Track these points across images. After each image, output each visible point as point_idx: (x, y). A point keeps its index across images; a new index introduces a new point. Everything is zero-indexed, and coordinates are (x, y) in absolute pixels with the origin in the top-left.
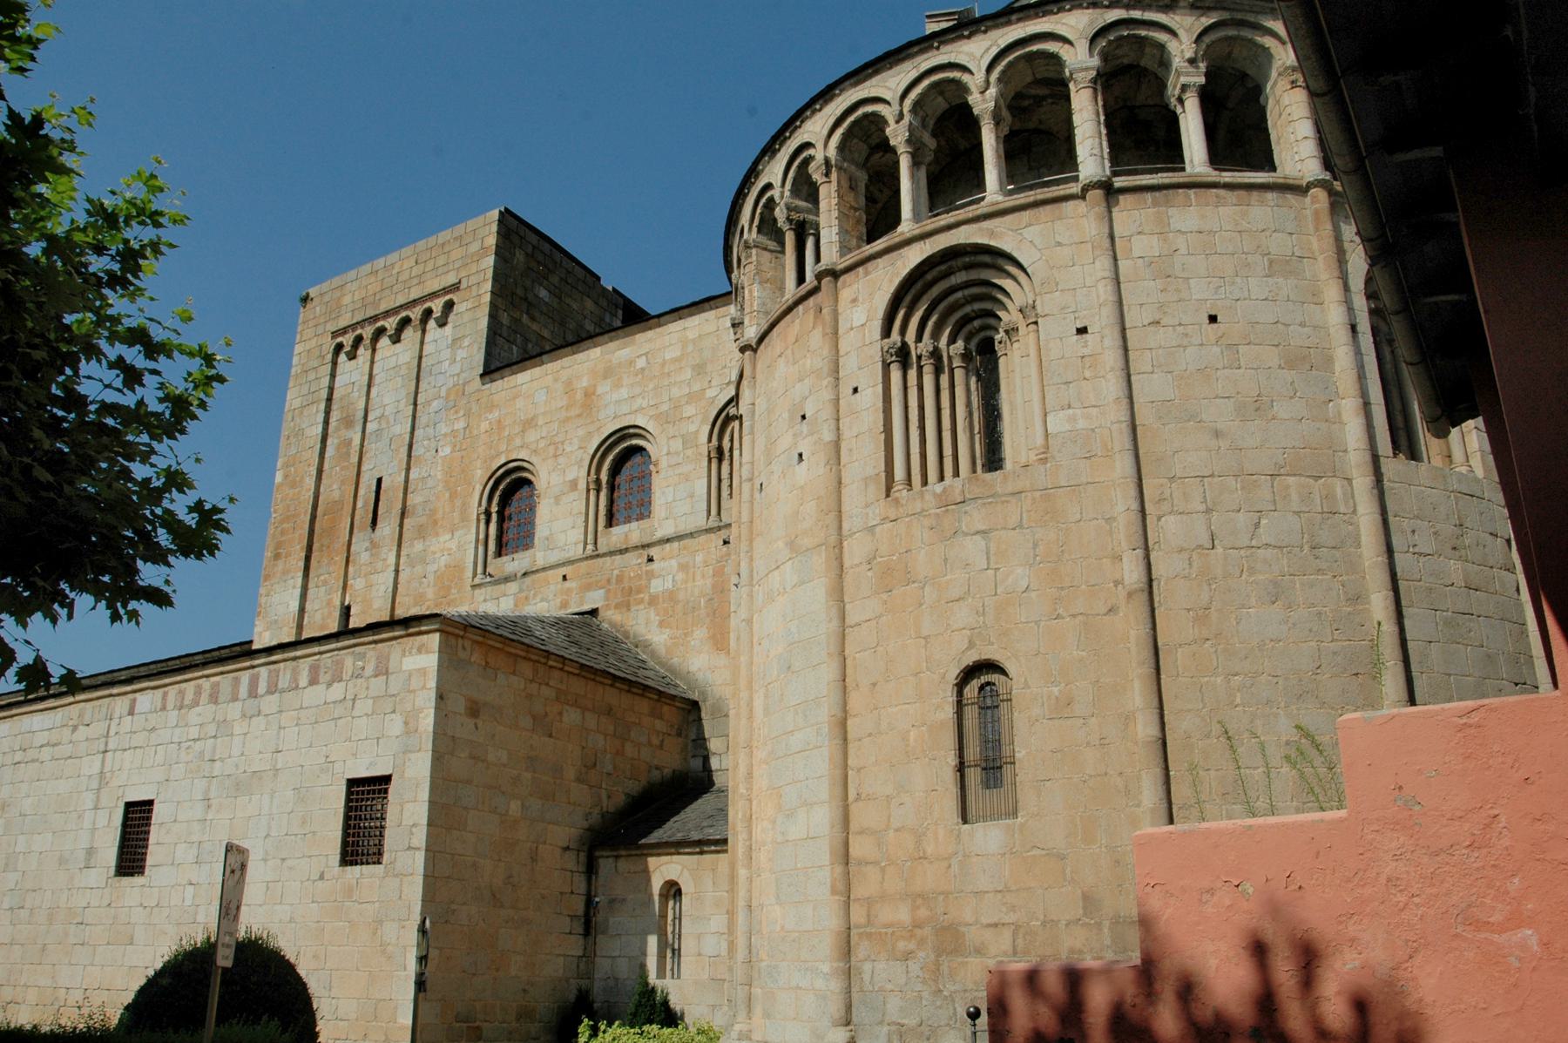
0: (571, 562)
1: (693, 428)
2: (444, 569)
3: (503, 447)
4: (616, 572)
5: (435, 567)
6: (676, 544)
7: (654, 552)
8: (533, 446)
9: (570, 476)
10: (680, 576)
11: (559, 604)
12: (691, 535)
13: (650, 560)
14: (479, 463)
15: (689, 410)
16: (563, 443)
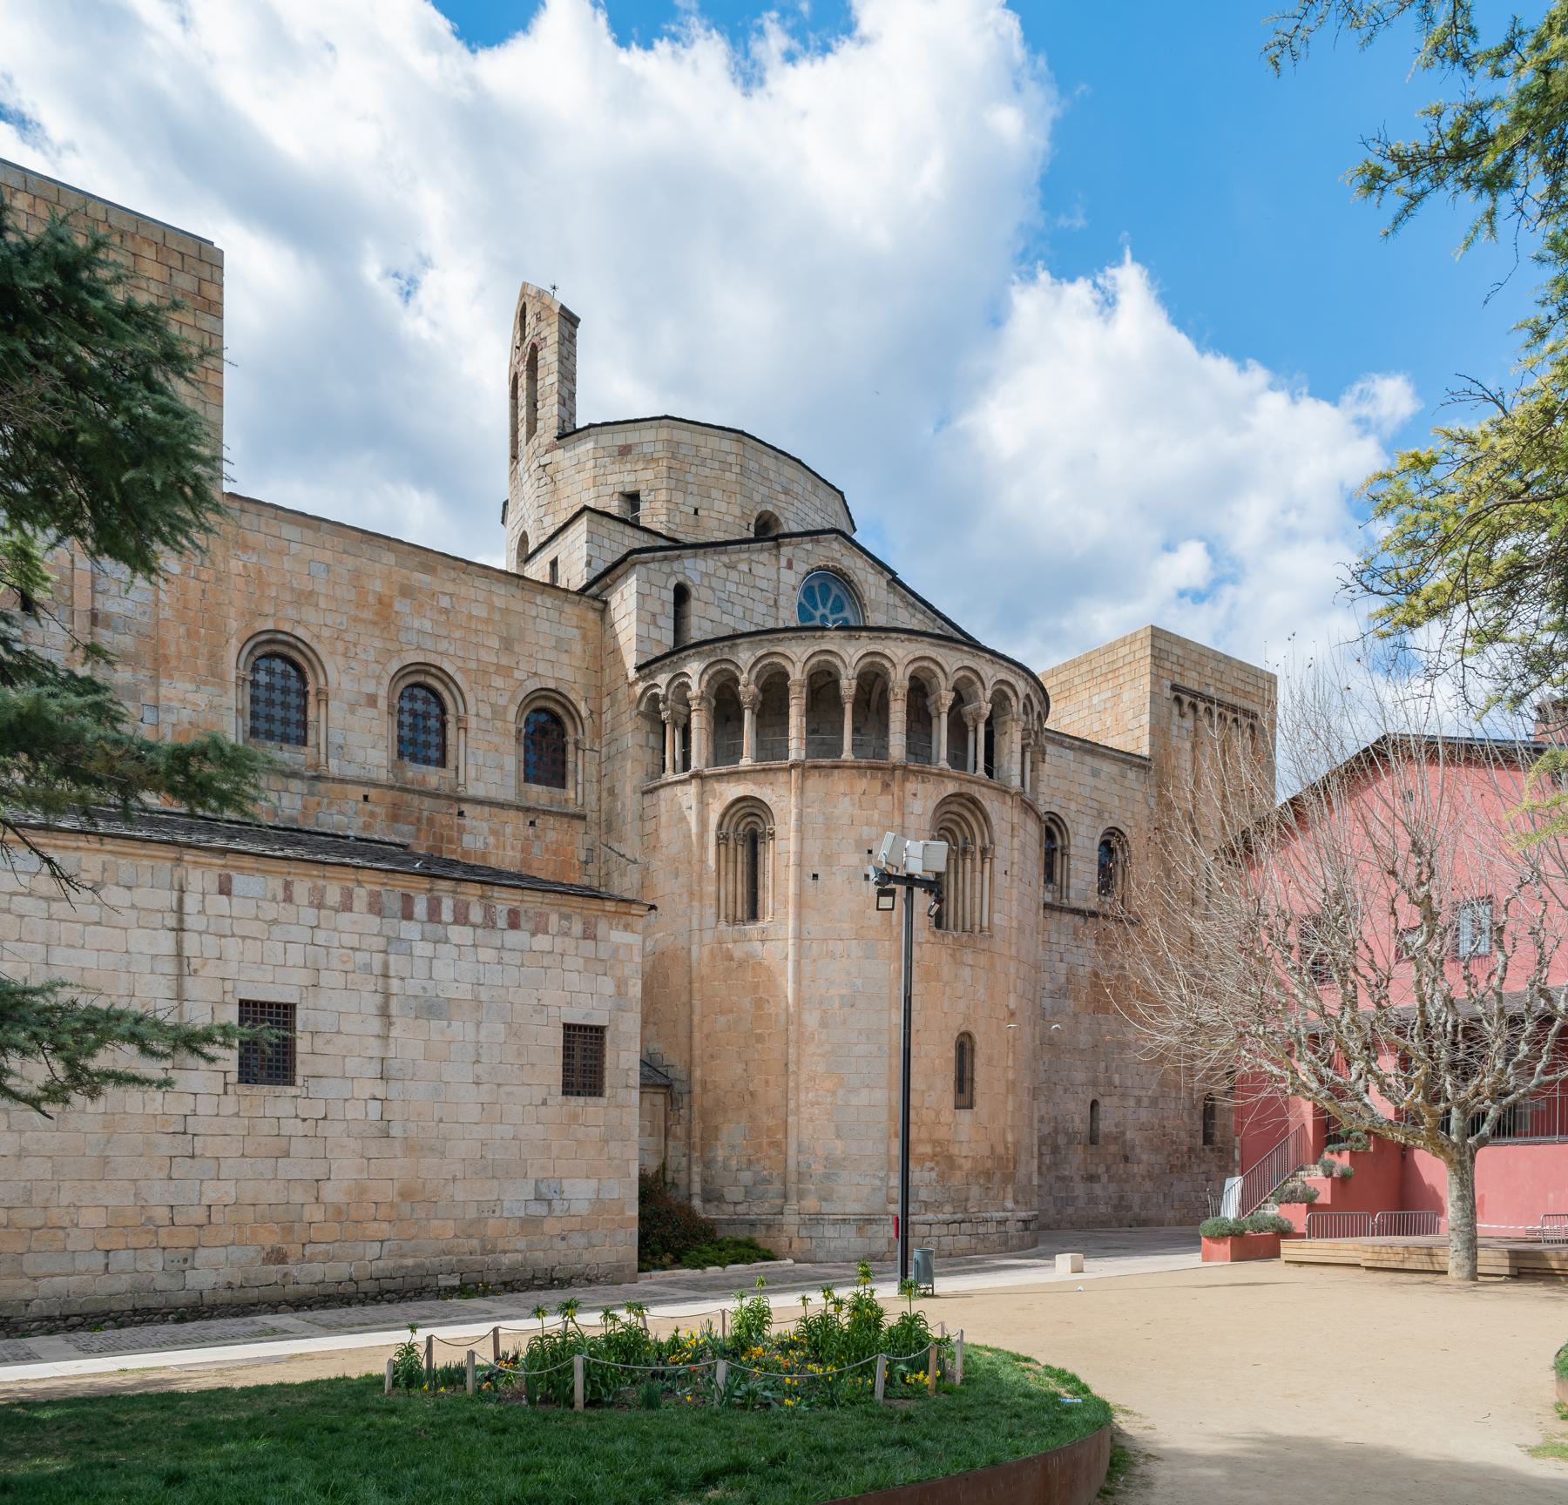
0: (374, 784)
1: (502, 701)
2: (186, 726)
3: (268, 608)
4: (425, 813)
5: (173, 718)
6: (486, 809)
7: (465, 807)
8: (316, 630)
9: (370, 687)
10: (491, 840)
11: (361, 824)
12: (502, 806)
13: (461, 814)
14: (232, 612)
15: (498, 682)
16: (355, 645)
